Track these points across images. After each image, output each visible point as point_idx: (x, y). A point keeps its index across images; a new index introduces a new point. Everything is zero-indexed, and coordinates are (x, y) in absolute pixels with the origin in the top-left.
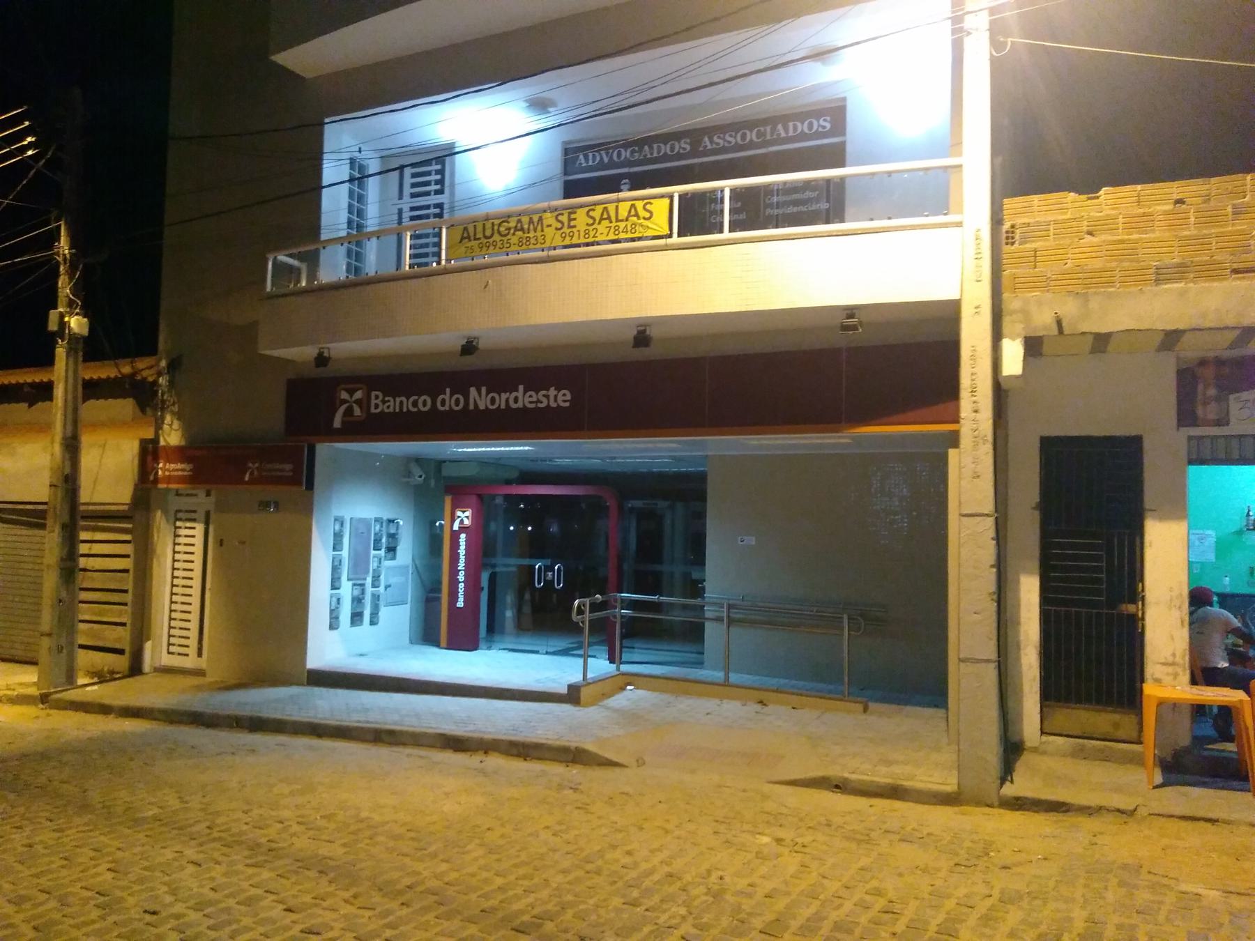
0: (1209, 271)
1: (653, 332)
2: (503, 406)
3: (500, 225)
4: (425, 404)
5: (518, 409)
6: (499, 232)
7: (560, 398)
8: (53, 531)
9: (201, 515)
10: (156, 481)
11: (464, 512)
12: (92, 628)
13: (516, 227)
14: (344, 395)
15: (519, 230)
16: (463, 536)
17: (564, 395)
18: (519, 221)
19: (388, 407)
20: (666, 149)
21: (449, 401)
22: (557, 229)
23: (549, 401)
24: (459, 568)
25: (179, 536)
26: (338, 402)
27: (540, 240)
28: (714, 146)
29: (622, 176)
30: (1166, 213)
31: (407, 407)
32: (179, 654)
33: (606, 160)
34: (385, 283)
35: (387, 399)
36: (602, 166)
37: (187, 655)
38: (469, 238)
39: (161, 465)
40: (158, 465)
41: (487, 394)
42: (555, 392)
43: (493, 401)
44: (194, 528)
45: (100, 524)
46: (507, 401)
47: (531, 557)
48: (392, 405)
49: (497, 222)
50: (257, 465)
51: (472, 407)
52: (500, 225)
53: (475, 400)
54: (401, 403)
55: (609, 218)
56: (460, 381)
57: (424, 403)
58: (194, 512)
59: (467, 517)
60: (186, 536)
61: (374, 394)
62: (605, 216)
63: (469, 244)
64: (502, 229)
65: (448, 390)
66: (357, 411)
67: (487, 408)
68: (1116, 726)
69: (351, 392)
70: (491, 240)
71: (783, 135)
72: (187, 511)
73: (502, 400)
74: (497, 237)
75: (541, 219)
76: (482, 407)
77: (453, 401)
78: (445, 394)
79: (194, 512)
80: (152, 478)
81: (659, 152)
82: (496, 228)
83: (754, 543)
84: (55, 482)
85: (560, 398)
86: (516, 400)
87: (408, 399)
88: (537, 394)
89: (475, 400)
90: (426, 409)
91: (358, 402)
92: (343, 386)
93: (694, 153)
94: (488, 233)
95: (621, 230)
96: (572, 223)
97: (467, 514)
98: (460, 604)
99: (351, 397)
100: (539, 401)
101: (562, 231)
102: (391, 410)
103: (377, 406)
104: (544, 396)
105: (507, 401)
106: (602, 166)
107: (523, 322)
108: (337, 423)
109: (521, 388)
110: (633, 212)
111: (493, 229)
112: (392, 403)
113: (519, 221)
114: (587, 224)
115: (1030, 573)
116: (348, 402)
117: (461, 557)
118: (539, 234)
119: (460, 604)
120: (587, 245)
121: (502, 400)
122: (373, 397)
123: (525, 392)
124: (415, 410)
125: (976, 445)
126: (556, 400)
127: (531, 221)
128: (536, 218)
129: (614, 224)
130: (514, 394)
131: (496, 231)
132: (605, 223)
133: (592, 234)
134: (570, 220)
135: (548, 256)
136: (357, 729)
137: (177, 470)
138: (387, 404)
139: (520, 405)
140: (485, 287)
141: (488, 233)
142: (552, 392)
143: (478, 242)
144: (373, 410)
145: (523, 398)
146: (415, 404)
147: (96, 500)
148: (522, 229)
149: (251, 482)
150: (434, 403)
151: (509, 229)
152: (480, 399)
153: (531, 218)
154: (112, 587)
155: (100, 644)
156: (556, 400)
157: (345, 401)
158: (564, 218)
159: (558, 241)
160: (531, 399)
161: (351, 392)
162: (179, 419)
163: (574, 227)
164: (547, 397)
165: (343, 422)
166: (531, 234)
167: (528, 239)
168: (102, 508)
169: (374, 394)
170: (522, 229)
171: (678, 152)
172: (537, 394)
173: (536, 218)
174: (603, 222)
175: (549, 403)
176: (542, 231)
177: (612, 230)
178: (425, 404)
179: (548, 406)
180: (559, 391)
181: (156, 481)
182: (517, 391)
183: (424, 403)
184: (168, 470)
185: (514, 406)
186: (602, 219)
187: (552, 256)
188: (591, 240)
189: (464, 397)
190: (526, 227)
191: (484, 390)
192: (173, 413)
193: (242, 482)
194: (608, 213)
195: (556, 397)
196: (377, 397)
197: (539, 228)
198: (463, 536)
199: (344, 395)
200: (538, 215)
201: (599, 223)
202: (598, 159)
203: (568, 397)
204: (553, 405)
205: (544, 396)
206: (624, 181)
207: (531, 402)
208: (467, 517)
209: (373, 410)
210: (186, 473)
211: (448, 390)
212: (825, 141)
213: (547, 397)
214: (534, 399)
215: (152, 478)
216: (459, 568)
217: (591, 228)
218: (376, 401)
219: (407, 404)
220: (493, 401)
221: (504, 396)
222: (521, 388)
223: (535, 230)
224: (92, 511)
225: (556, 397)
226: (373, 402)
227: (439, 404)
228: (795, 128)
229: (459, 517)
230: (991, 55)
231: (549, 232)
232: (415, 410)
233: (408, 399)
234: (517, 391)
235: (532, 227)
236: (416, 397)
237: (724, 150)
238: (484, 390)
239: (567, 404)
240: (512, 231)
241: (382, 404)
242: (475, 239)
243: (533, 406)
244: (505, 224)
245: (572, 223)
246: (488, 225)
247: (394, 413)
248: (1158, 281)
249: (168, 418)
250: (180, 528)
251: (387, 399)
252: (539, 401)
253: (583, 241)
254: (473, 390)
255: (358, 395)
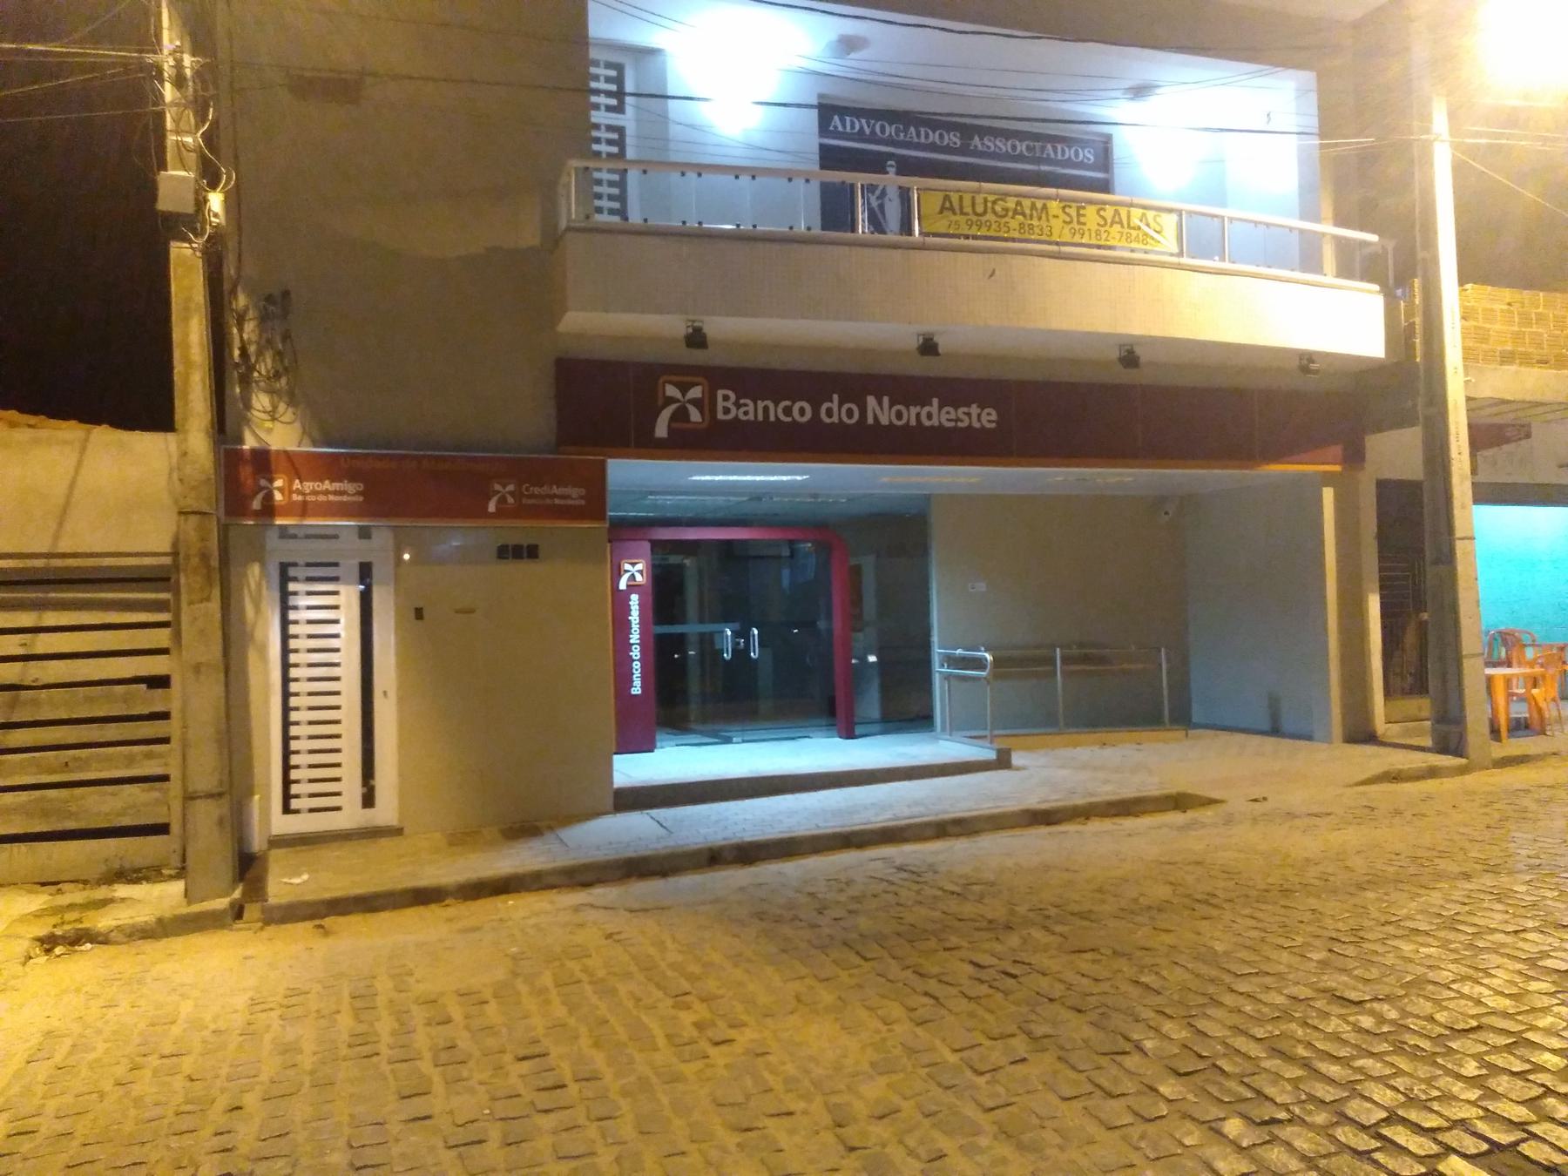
0: (1526, 360)
1: (1143, 354)
2: (913, 422)
3: (994, 202)
4: (802, 412)
5: (932, 427)
6: (994, 212)
7: (984, 418)
8: (208, 599)
9: (350, 566)
10: (269, 510)
11: (633, 564)
12: (42, 799)
13: (1016, 210)
14: (671, 391)
15: (1019, 214)
16: (634, 598)
17: (989, 414)
18: (1019, 203)
19: (746, 413)
20: (934, 137)
21: (836, 411)
22: (1064, 222)
23: (970, 419)
24: (632, 641)
25: (295, 608)
26: (660, 402)
27: (1046, 230)
28: (985, 149)
29: (891, 156)
30: (1502, 311)
31: (776, 416)
32: (312, 810)
33: (867, 131)
34: (951, 253)
35: (742, 401)
36: (860, 136)
37: (338, 809)
38: (952, 209)
39: (278, 483)
40: (271, 481)
41: (890, 408)
42: (979, 410)
43: (899, 415)
44: (336, 593)
45: (53, 595)
46: (918, 415)
47: (714, 621)
48: (750, 411)
49: (991, 198)
50: (511, 488)
51: (870, 421)
52: (994, 202)
53: (882, 409)
54: (766, 409)
55: (1121, 223)
56: (906, 389)
57: (801, 412)
58: (336, 565)
59: (641, 572)
60: (309, 608)
61: (720, 393)
62: (947, 205)
63: (954, 218)
64: (998, 208)
65: (835, 397)
66: (695, 415)
67: (891, 422)
68: (1420, 709)
69: (684, 388)
70: (984, 219)
71: (840, 129)
72: (308, 565)
73: (911, 414)
74: (990, 216)
75: (1045, 207)
76: (884, 421)
77: (780, 410)
78: (831, 401)
79: (336, 565)
80: (256, 504)
81: (1063, 155)
82: (989, 205)
83: (984, 589)
84: (192, 503)
85: (986, 418)
86: (929, 416)
87: (776, 406)
88: (956, 411)
89: (882, 409)
90: (805, 419)
91: (697, 403)
92: (665, 378)
93: (964, 150)
94: (980, 209)
95: (1133, 238)
96: (1082, 219)
97: (639, 567)
98: (636, 690)
99: (684, 396)
100: (957, 420)
101: (1070, 226)
102: (751, 417)
103: (727, 411)
104: (964, 413)
105: (918, 415)
106: (860, 136)
107: (1042, 325)
108: (661, 430)
109: (935, 401)
110: (947, 205)
111: (986, 206)
112: (751, 408)
113: (1019, 203)
114: (1098, 224)
115: (1373, 592)
116: (678, 401)
117: (633, 626)
118: (1044, 223)
119: (636, 690)
120: (1099, 247)
121: (911, 414)
122: (720, 398)
123: (940, 408)
124: (789, 419)
125: (1462, 482)
126: (979, 420)
127: (1033, 207)
128: (1039, 204)
129: (1127, 230)
130: (927, 409)
131: (989, 210)
132: (1117, 227)
133: (1104, 236)
134: (1079, 215)
135: (1060, 252)
136: (909, 826)
137: (327, 492)
138: (743, 409)
139: (935, 422)
140: (991, 276)
141: (980, 209)
142: (974, 410)
143: (966, 218)
144: (720, 416)
145: (937, 415)
146: (787, 411)
147: (64, 547)
148: (1023, 214)
149: (500, 513)
150: (816, 412)
151: (1006, 210)
152: (880, 411)
153: (1116, 211)
154: (101, 714)
155: (71, 825)
156: (979, 420)
157: (671, 400)
158: (1073, 212)
159: (1067, 237)
160: (947, 416)
161: (684, 388)
162: (292, 402)
163: (1084, 224)
164: (969, 414)
165: (670, 430)
166: (1035, 222)
167: (1031, 227)
168: (90, 562)
169: (720, 393)
170: (1023, 214)
171: (948, 144)
172: (956, 411)
173: (1039, 204)
174: (1115, 226)
175: (971, 423)
176: (1048, 220)
177: (1125, 237)
178: (802, 412)
179: (970, 427)
180: (983, 409)
181: (269, 510)
182: (931, 405)
183: (801, 412)
184: (299, 492)
185: (927, 423)
186: (1113, 223)
187: (1065, 253)
188: (1102, 243)
189: (858, 406)
190: (1028, 212)
191: (886, 400)
192: (271, 392)
193: (485, 514)
194: (951, 202)
195: (979, 415)
196: (726, 398)
197: (1044, 216)
198: (634, 598)
199: (671, 391)
200: (1043, 201)
201: (1111, 226)
202: (857, 127)
203: (994, 417)
204: (976, 425)
205: (964, 413)
206: (889, 163)
207: (948, 420)
208: (641, 572)
209: (720, 416)
210: (345, 498)
211: (835, 397)
212: (1000, 164)
213: (969, 414)
214: (953, 416)
215: (256, 504)
216: (632, 641)
217: (1103, 229)
218: (726, 404)
219: (776, 412)
220: (899, 415)
221: (914, 410)
222: (935, 401)
223: (1040, 219)
224: (110, 568)
225: (979, 415)
226: (720, 403)
227: (823, 415)
228: (927, 136)
229: (627, 571)
230: (1453, 155)
231: (1056, 224)
232: (789, 419)
233: (776, 406)
234: (931, 405)
235: (1034, 212)
236: (788, 403)
237: (982, 155)
238: (886, 400)
239: (993, 425)
240: (1010, 214)
241: (728, 405)
242: (962, 213)
243: (952, 424)
244: (1000, 202)
245: (1082, 219)
246: (979, 199)
247: (755, 423)
248: (1502, 363)
249: (261, 401)
250: (295, 593)
251: (742, 401)
252: (957, 420)
253: (1094, 242)
254: (871, 401)
255: (695, 392)
